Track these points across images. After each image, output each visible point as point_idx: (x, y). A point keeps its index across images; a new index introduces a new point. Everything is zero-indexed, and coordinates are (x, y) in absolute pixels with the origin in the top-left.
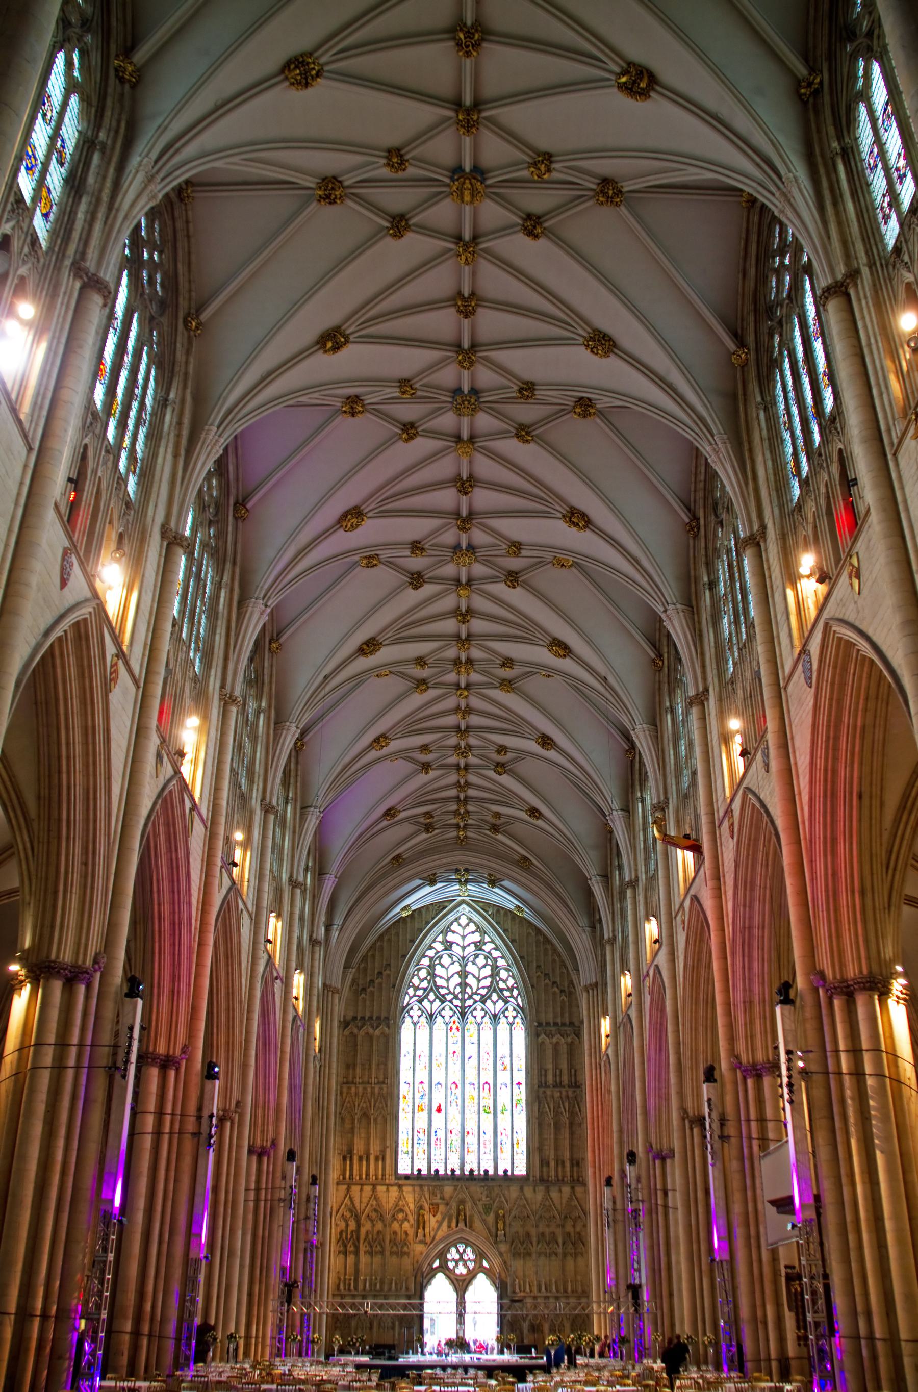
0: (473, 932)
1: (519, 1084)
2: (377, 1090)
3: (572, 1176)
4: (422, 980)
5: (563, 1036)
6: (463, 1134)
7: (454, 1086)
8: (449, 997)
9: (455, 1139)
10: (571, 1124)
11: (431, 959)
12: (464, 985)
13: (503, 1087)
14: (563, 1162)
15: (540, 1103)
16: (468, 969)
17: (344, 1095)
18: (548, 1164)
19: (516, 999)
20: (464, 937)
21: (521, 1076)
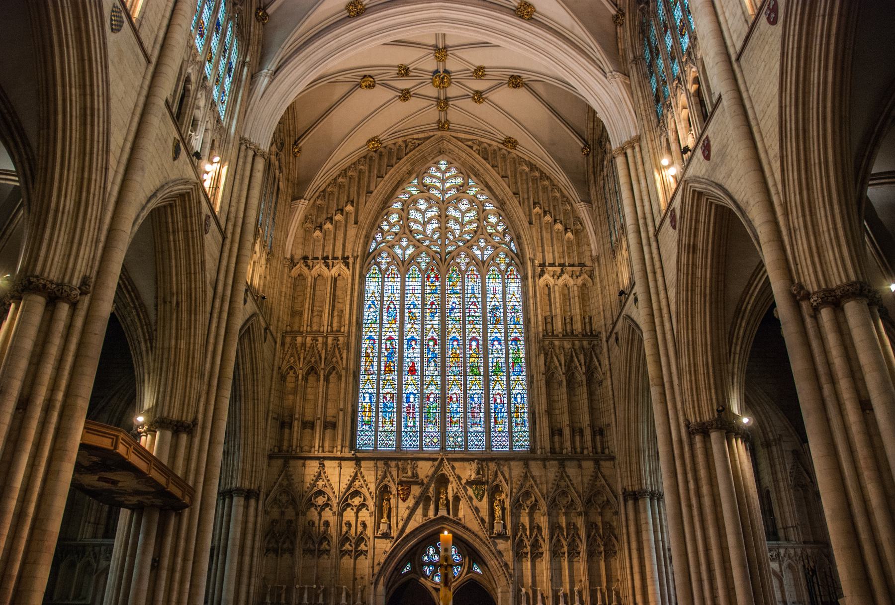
0: (455, 177)
1: (516, 340)
2: (330, 340)
3: (594, 447)
4: (392, 226)
5: (572, 277)
6: (444, 399)
7: (431, 343)
8: (427, 243)
9: (433, 406)
10: (590, 381)
11: (404, 203)
12: (443, 230)
13: (496, 343)
14: (581, 431)
15: (546, 355)
16: (450, 214)
17: (287, 346)
18: (560, 433)
19: (508, 245)
20: (443, 181)
21: (517, 331)
